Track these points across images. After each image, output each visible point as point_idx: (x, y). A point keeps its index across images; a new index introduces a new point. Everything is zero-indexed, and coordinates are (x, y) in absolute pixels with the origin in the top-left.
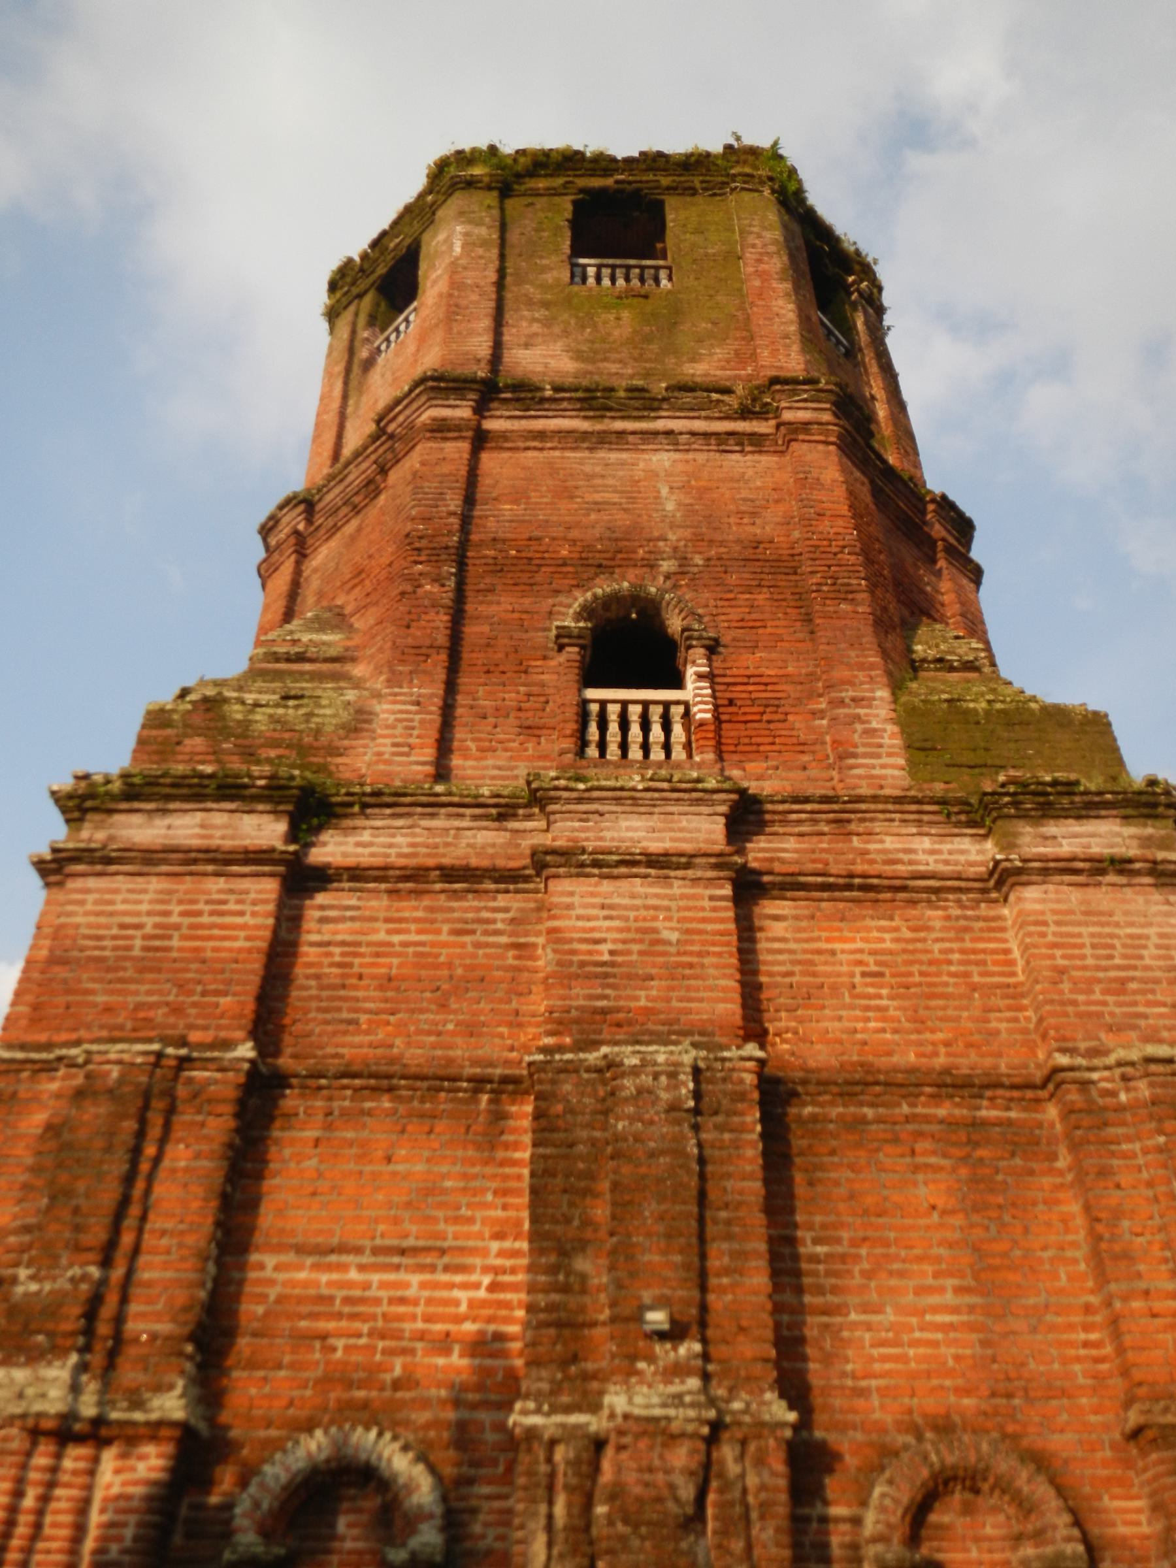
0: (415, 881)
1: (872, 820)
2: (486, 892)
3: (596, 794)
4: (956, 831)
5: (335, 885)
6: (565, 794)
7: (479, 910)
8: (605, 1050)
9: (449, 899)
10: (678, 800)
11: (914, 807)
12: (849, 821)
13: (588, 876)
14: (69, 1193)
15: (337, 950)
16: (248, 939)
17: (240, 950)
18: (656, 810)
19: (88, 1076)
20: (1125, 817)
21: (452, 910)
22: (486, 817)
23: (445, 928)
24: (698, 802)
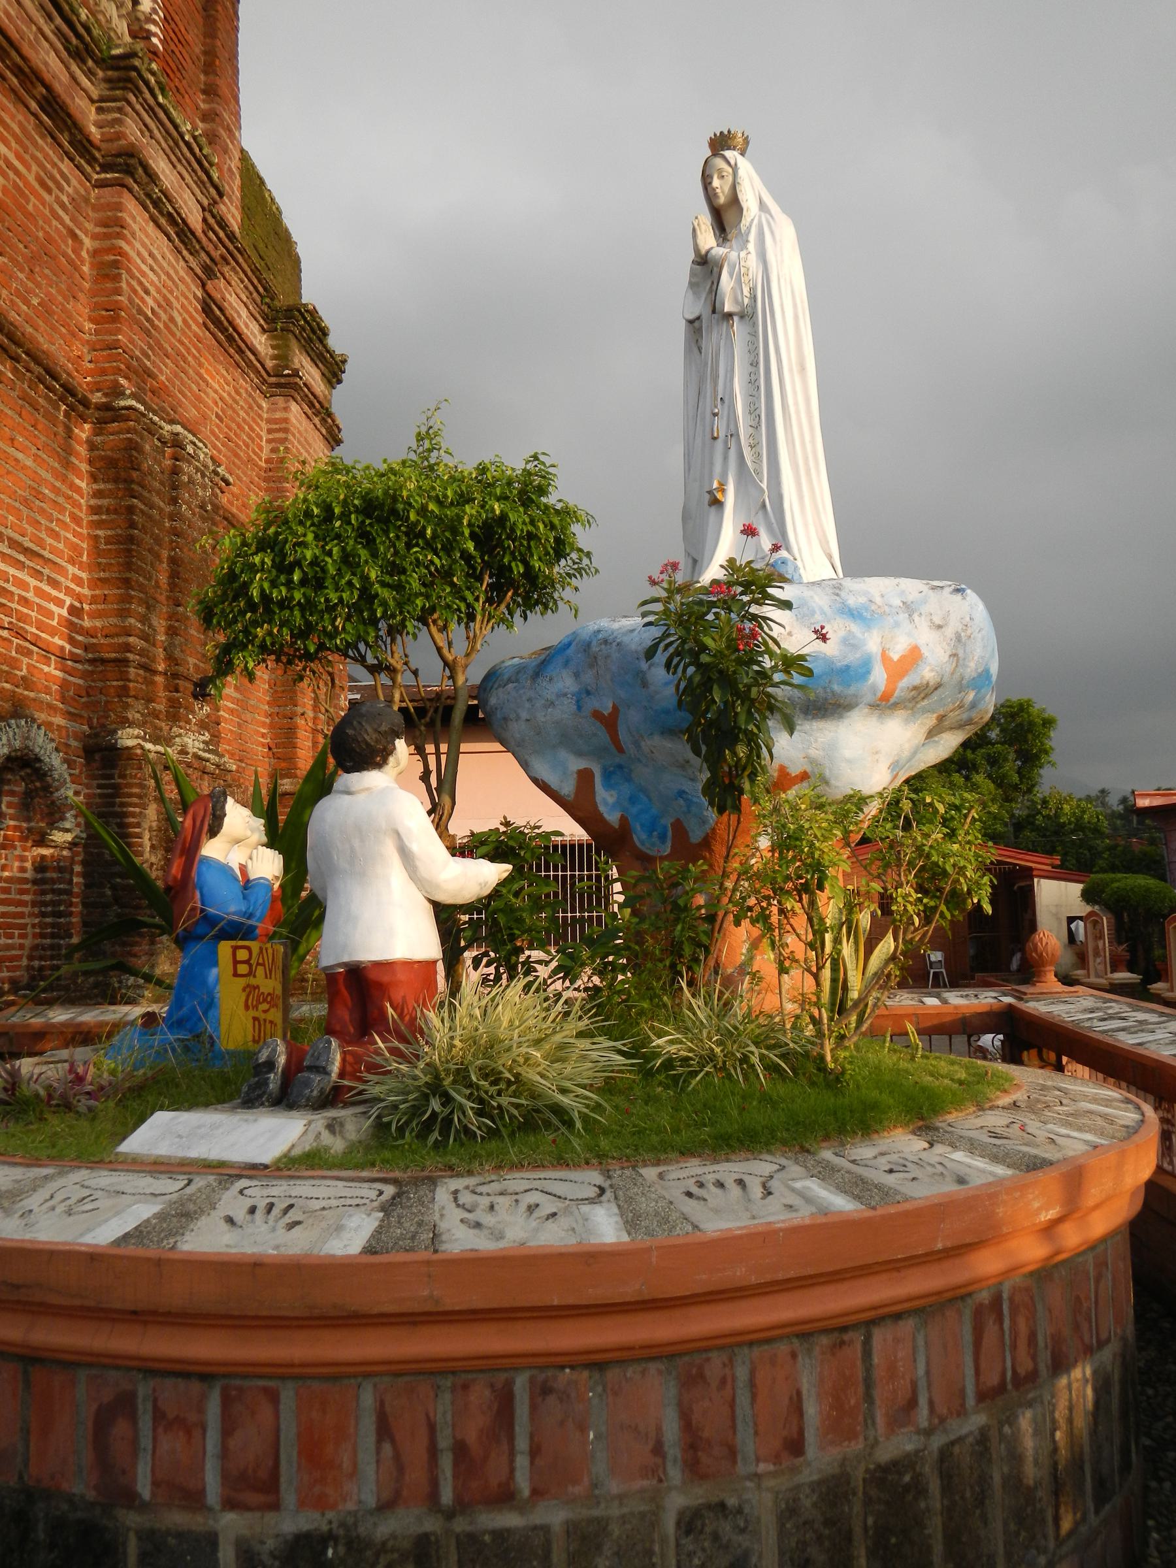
1: (236, 273)
2: (60, 145)
3: (162, 115)
4: (258, 316)
6: (148, 95)
7: (54, 165)
8: (178, 428)
9: (36, 128)
10: (193, 170)
11: (255, 281)
12: (228, 263)
13: (145, 208)
18: (179, 167)
20: (323, 374)
23: (34, 168)
24: (200, 183)
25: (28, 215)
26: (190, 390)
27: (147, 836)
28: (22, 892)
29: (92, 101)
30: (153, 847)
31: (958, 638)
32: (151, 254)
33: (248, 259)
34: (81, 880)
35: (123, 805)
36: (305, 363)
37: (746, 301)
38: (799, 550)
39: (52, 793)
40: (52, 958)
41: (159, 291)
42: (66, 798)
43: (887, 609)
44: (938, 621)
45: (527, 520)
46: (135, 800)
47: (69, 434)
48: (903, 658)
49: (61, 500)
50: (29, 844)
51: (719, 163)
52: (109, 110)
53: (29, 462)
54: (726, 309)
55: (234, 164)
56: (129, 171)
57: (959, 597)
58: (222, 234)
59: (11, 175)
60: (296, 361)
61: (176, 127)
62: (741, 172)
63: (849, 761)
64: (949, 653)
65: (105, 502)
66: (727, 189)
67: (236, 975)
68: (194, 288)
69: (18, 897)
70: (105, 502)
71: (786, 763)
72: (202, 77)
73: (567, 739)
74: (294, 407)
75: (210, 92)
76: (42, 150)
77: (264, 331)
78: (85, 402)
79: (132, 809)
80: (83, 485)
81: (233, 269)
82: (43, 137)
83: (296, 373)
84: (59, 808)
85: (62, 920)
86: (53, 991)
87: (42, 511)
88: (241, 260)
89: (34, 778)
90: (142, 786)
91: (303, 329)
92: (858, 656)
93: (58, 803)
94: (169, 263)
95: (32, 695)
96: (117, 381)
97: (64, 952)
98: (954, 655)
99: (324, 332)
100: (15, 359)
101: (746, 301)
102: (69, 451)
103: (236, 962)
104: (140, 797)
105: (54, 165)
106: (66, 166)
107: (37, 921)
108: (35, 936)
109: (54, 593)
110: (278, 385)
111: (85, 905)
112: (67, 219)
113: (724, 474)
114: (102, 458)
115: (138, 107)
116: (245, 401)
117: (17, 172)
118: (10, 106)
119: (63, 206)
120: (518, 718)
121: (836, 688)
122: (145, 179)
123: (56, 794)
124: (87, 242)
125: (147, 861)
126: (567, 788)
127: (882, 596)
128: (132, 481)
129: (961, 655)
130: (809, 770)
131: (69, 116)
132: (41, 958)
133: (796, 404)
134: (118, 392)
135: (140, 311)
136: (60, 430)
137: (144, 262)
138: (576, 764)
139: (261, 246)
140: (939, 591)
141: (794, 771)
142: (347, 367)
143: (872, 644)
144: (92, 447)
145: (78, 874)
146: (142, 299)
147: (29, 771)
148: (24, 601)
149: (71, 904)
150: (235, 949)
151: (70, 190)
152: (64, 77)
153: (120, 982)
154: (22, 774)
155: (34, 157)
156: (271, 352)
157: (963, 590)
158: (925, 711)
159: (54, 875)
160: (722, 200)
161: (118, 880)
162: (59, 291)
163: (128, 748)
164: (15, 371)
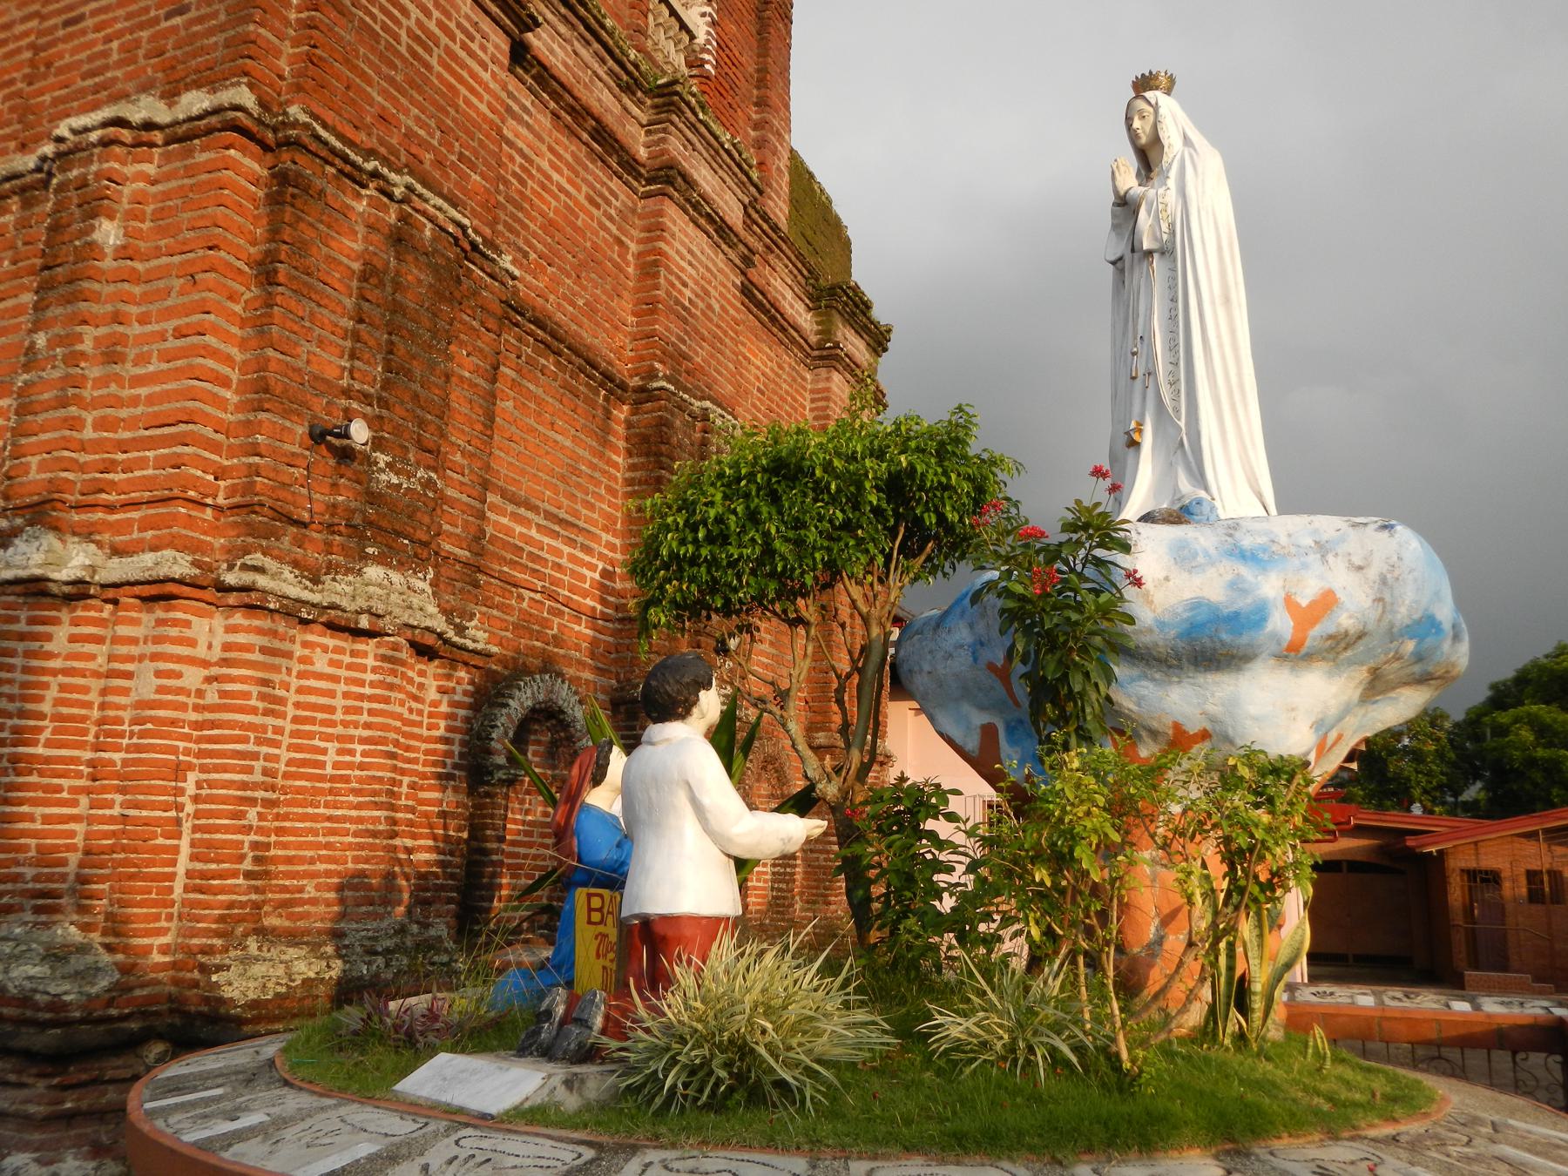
0: (574, 119)
1: (781, 260)
2: (609, 167)
3: (703, 129)
5: (520, 71)
6: (689, 114)
7: (603, 184)
8: (708, 404)
12: (772, 252)
14: (408, 374)
15: (518, 159)
16: (489, 105)
17: (485, 118)
19: (404, 218)
21: (586, 168)
22: (617, 78)
23: (584, 188)
24: (741, 184)
25: (576, 229)
26: (727, 368)
28: (543, 835)
29: (643, 126)
31: (1384, 581)
32: (690, 251)
33: (791, 245)
36: (848, 335)
37: (1165, 237)
38: (1219, 489)
41: (697, 283)
43: (1293, 550)
44: (1357, 561)
45: (939, 470)
47: (608, 415)
48: (1313, 604)
49: (597, 475)
51: (1140, 104)
52: (657, 131)
53: (568, 443)
54: (1145, 247)
55: (783, 163)
56: (670, 181)
57: (1386, 534)
58: (765, 227)
59: (563, 197)
60: (839, 334)
61: (716, 138)
62: (1162, 111)
63: (1255, 719)
64: (1372, 597)
65: (638, 474)
66: (1148, 129)
67: (590, 922)
68: (732, 277)
70: (638, 474)
71: (1181, 720)
72: (755, 92)
73: (967, 693)
74: (836, 377)
75: (762, 103)
76: (593, 173)
77: (810, 309)
78: (623, 386)
80: (620, 460)
81: (778, 257)
82: (593, 162)
83: (837, 346)
87: (578, 486)
88: (784, 247)
91: (846, 304)
92: (1249, 601)
94: (708, 257)
95: (562, 652)
96: (652, 366)
98: (1380, 600)
99: (867, 306)
100: (558, 353)
101: (1165, 237)
102: (607, 430)
103: (590, 910)
105: (603, 184)
106: (615, 184)
109: (587, 558)
110: (821, 358)
112: (614, 229)
113: (1143, 415)
114: (637, 435)
115: (681, 125)
116: (789, 375)
117: (567, 194)
118: (565, 140)
119: (611, 218)
120: (921, 670)
121: (1225, 636)
122: (684, 186)
123: (579, 744)
124: (633, 247)
126: (972, 743)
127: (1289, 535)
128: (662, 454)
129: (1388, 598)
130: (1209, 727)
131: (617, 141)
133: (1219, 336)
134: (652, 375)
135: (678, 302)
136: (600, 412)
137: (682, 258)
138: (979, 719)
139: (809, 233)
140: (1361, 529)
141: (1193, 728)
142: (892, 336)
143: (1270, 587)
144: (629, 425)
146: (680, 292)
148: (558, 567)
150: (589, 896)
151: (618, 204)
152: (617, 109)
155: (584, 180)
156: (815, 327)
157: (1392, 527)
158: (1351, 663)
160: (1144, 140)
162: (605, 292)
164: (557, 364)
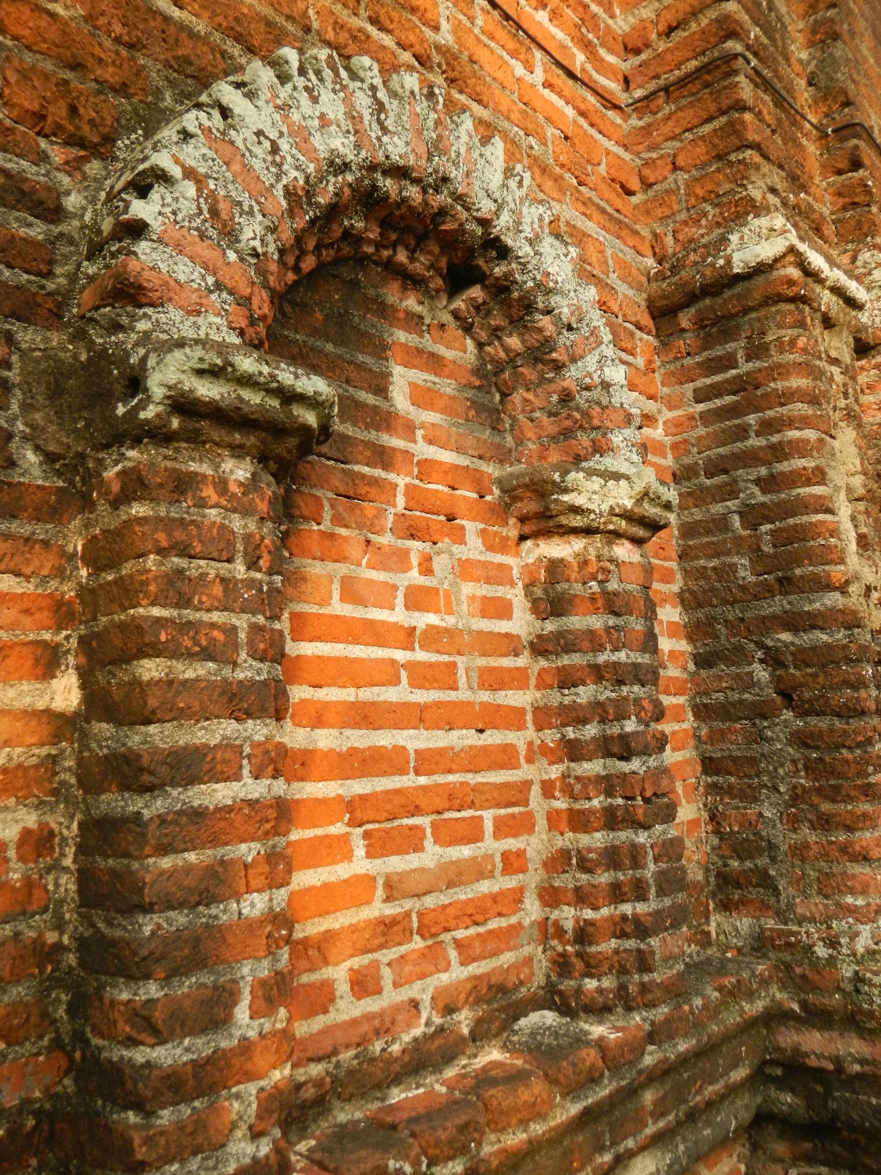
27: (845, 510)
30: (862, 540)
34: (683, 646)
35: (768, 427)
39: (558, 367)
40: (617, 894)
42: (606, 386)
46: (800, 408)
50: (512, 531)
69: (485, 696)
79: (793, 434)
84: (586, 415)
85: (635, 764)
86: (629, 1009)
89: (497, 320)
90: (817, 374)
93: (581, 399)
97: (651, 869)
104: (814, 400)
107: (555, 772)
108: (553, 818)
111: (702, 712)
123: (573, 372)
125: (857, 578)
132: (581, 897)
145: (673, 631)
147: (476, 292)
149: (659, 714)
153: (833, 943)
154: (459, 304)
159: (596, 622)
161: (786, 636)
163: (761, 269)
